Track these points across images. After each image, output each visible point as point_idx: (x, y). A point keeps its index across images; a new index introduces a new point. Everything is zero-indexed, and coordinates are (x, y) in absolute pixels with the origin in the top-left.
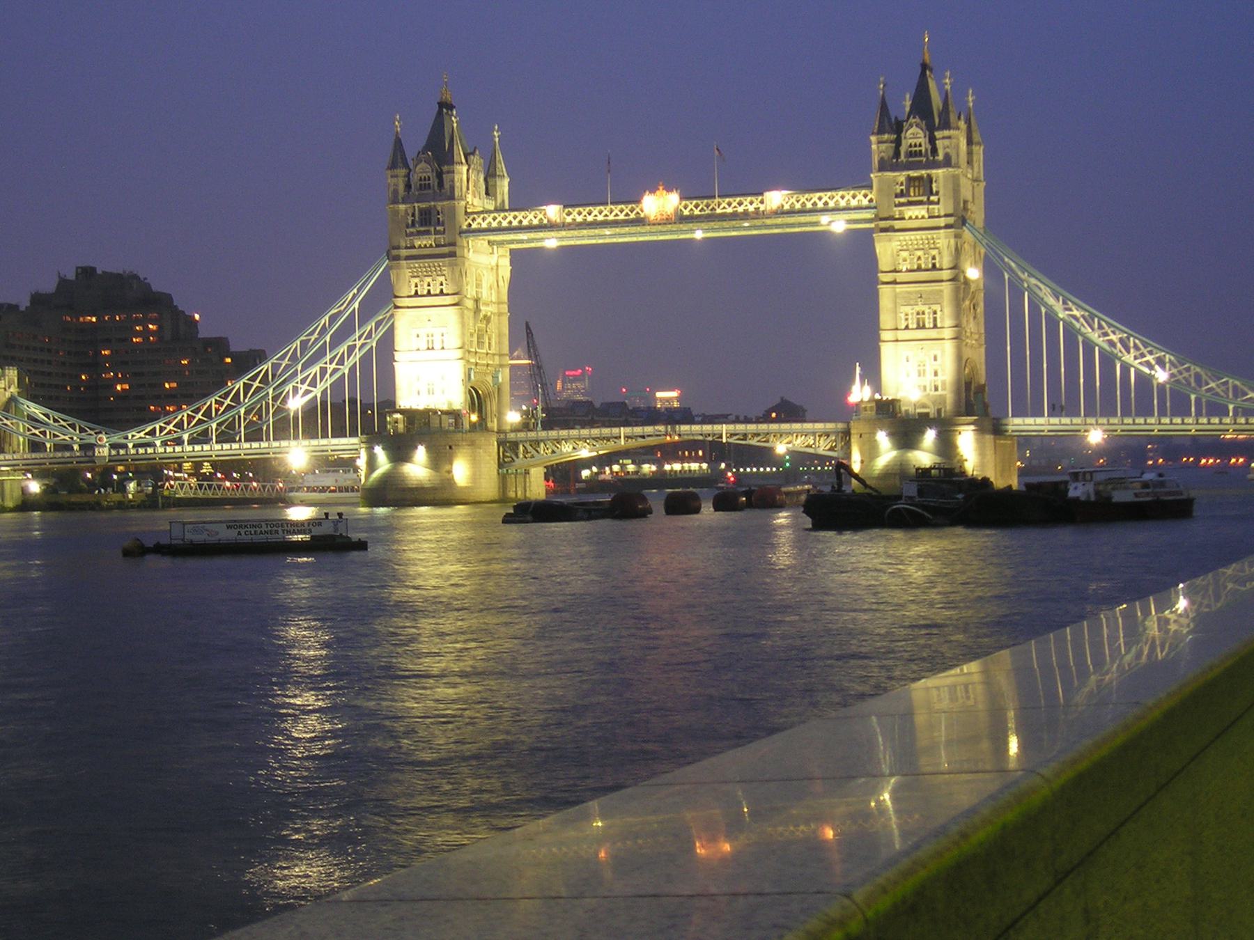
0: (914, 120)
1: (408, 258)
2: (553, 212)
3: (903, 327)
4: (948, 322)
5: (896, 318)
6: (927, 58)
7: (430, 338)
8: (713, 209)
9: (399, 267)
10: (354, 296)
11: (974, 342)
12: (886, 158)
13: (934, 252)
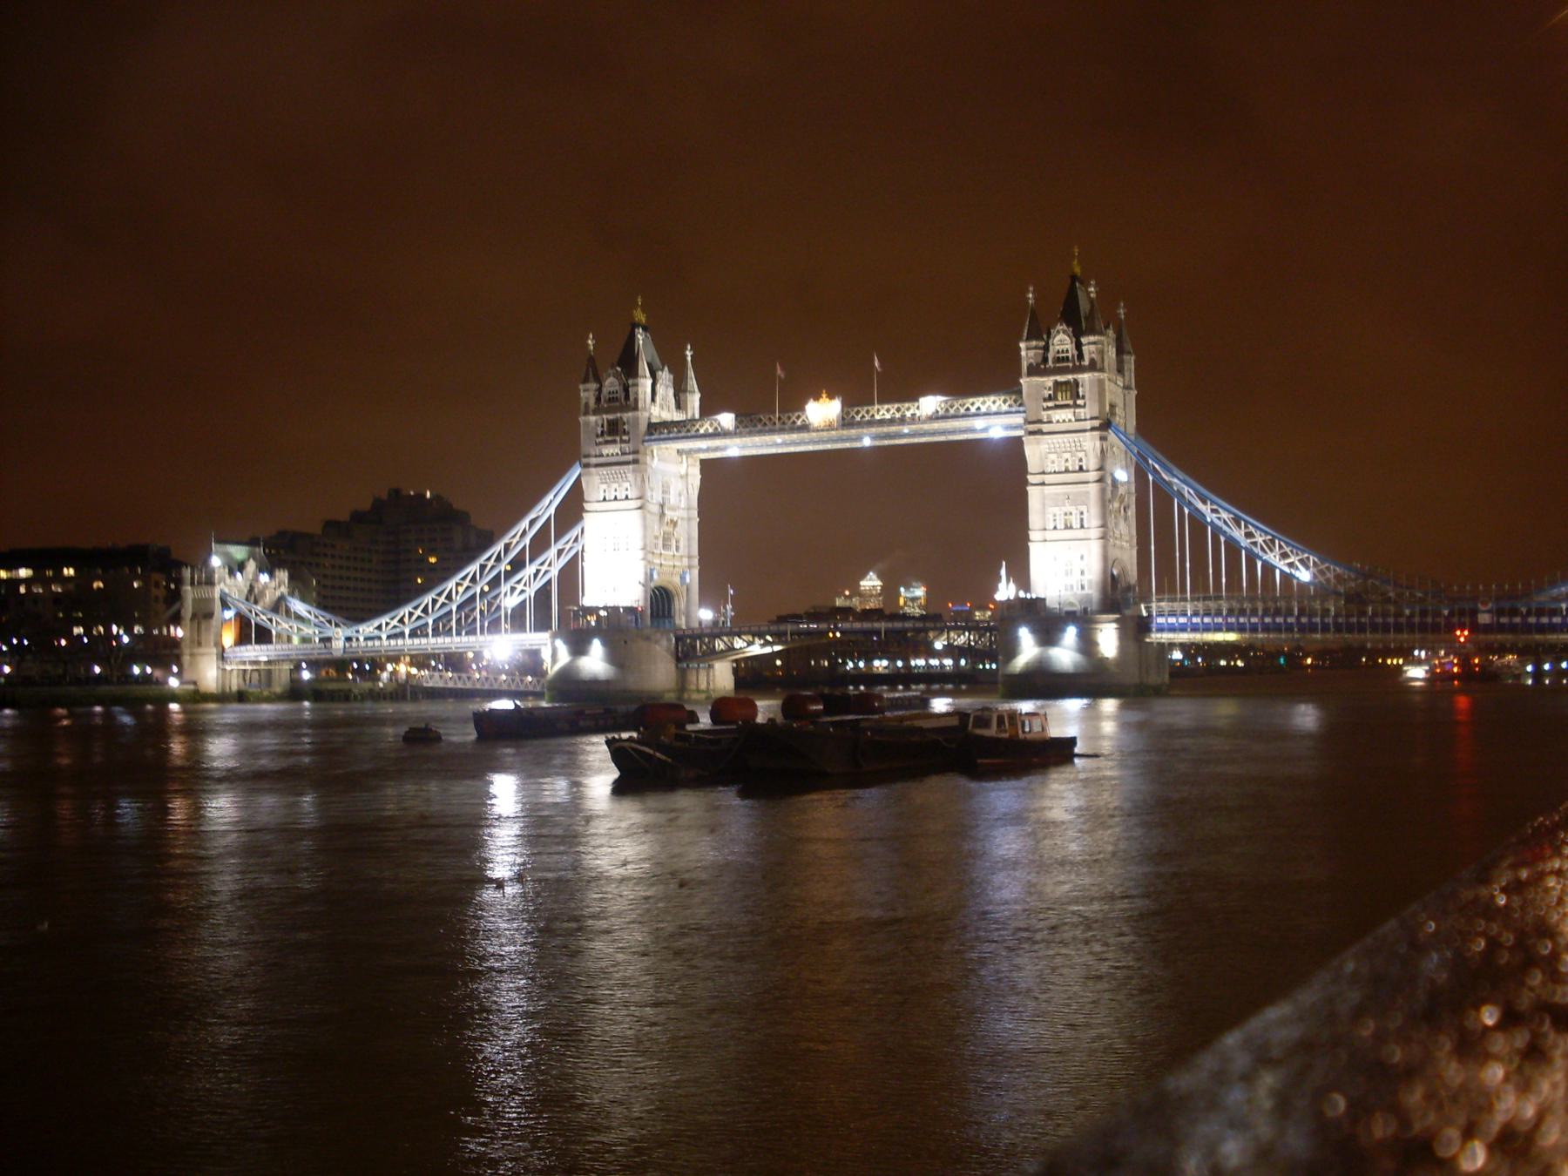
0: (1061, 327)
1: (597, 465)
2: (727, 420)
3: (1052, 527)
4: (1093, 520)
6: (1078, 270)
8: (873, 416)
9: (586, 474)
11: (1125, 544)
13: (1081, 455)
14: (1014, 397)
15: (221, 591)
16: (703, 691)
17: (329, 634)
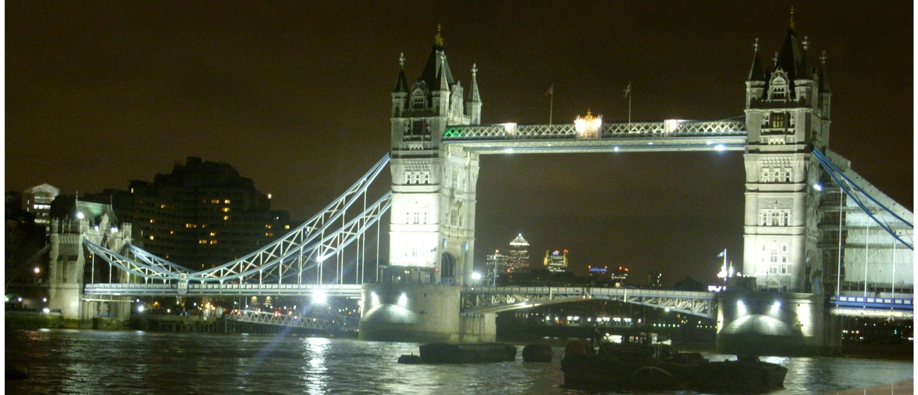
0: (779, 71)
1: (404, 157)
2: (510, 127)
3: (762, 224)
5: (757, 217)
6: (792, 25)
7: (417, 216)
8: (627, 131)
9: (397, 163)
10: (364, 183)
12: (756, 99)
13: (788, 170)
14: (738, 123)
15: (84, 238)
16: (476, 335)
17: (176, 276)
